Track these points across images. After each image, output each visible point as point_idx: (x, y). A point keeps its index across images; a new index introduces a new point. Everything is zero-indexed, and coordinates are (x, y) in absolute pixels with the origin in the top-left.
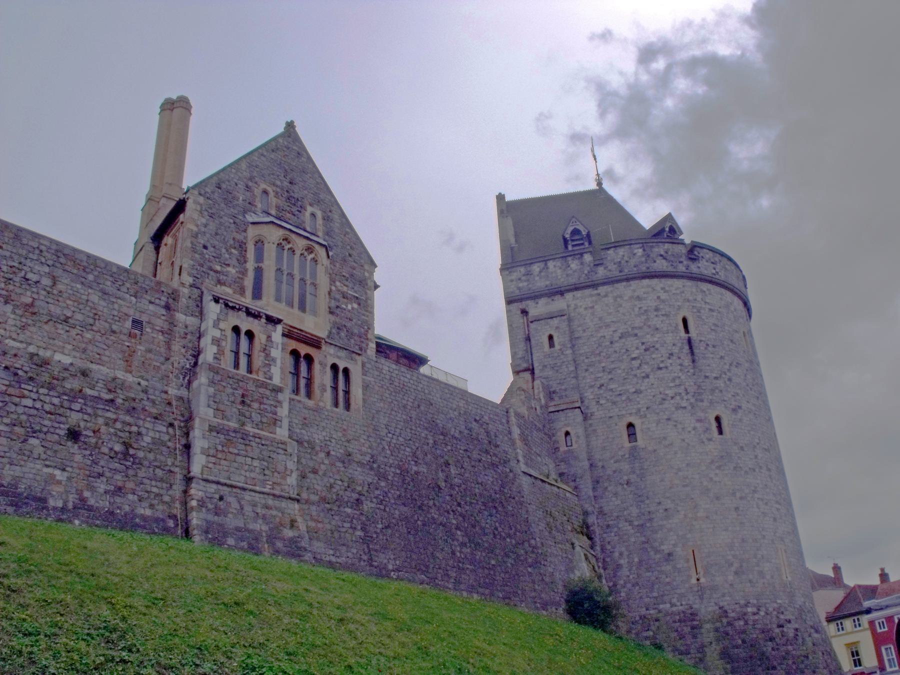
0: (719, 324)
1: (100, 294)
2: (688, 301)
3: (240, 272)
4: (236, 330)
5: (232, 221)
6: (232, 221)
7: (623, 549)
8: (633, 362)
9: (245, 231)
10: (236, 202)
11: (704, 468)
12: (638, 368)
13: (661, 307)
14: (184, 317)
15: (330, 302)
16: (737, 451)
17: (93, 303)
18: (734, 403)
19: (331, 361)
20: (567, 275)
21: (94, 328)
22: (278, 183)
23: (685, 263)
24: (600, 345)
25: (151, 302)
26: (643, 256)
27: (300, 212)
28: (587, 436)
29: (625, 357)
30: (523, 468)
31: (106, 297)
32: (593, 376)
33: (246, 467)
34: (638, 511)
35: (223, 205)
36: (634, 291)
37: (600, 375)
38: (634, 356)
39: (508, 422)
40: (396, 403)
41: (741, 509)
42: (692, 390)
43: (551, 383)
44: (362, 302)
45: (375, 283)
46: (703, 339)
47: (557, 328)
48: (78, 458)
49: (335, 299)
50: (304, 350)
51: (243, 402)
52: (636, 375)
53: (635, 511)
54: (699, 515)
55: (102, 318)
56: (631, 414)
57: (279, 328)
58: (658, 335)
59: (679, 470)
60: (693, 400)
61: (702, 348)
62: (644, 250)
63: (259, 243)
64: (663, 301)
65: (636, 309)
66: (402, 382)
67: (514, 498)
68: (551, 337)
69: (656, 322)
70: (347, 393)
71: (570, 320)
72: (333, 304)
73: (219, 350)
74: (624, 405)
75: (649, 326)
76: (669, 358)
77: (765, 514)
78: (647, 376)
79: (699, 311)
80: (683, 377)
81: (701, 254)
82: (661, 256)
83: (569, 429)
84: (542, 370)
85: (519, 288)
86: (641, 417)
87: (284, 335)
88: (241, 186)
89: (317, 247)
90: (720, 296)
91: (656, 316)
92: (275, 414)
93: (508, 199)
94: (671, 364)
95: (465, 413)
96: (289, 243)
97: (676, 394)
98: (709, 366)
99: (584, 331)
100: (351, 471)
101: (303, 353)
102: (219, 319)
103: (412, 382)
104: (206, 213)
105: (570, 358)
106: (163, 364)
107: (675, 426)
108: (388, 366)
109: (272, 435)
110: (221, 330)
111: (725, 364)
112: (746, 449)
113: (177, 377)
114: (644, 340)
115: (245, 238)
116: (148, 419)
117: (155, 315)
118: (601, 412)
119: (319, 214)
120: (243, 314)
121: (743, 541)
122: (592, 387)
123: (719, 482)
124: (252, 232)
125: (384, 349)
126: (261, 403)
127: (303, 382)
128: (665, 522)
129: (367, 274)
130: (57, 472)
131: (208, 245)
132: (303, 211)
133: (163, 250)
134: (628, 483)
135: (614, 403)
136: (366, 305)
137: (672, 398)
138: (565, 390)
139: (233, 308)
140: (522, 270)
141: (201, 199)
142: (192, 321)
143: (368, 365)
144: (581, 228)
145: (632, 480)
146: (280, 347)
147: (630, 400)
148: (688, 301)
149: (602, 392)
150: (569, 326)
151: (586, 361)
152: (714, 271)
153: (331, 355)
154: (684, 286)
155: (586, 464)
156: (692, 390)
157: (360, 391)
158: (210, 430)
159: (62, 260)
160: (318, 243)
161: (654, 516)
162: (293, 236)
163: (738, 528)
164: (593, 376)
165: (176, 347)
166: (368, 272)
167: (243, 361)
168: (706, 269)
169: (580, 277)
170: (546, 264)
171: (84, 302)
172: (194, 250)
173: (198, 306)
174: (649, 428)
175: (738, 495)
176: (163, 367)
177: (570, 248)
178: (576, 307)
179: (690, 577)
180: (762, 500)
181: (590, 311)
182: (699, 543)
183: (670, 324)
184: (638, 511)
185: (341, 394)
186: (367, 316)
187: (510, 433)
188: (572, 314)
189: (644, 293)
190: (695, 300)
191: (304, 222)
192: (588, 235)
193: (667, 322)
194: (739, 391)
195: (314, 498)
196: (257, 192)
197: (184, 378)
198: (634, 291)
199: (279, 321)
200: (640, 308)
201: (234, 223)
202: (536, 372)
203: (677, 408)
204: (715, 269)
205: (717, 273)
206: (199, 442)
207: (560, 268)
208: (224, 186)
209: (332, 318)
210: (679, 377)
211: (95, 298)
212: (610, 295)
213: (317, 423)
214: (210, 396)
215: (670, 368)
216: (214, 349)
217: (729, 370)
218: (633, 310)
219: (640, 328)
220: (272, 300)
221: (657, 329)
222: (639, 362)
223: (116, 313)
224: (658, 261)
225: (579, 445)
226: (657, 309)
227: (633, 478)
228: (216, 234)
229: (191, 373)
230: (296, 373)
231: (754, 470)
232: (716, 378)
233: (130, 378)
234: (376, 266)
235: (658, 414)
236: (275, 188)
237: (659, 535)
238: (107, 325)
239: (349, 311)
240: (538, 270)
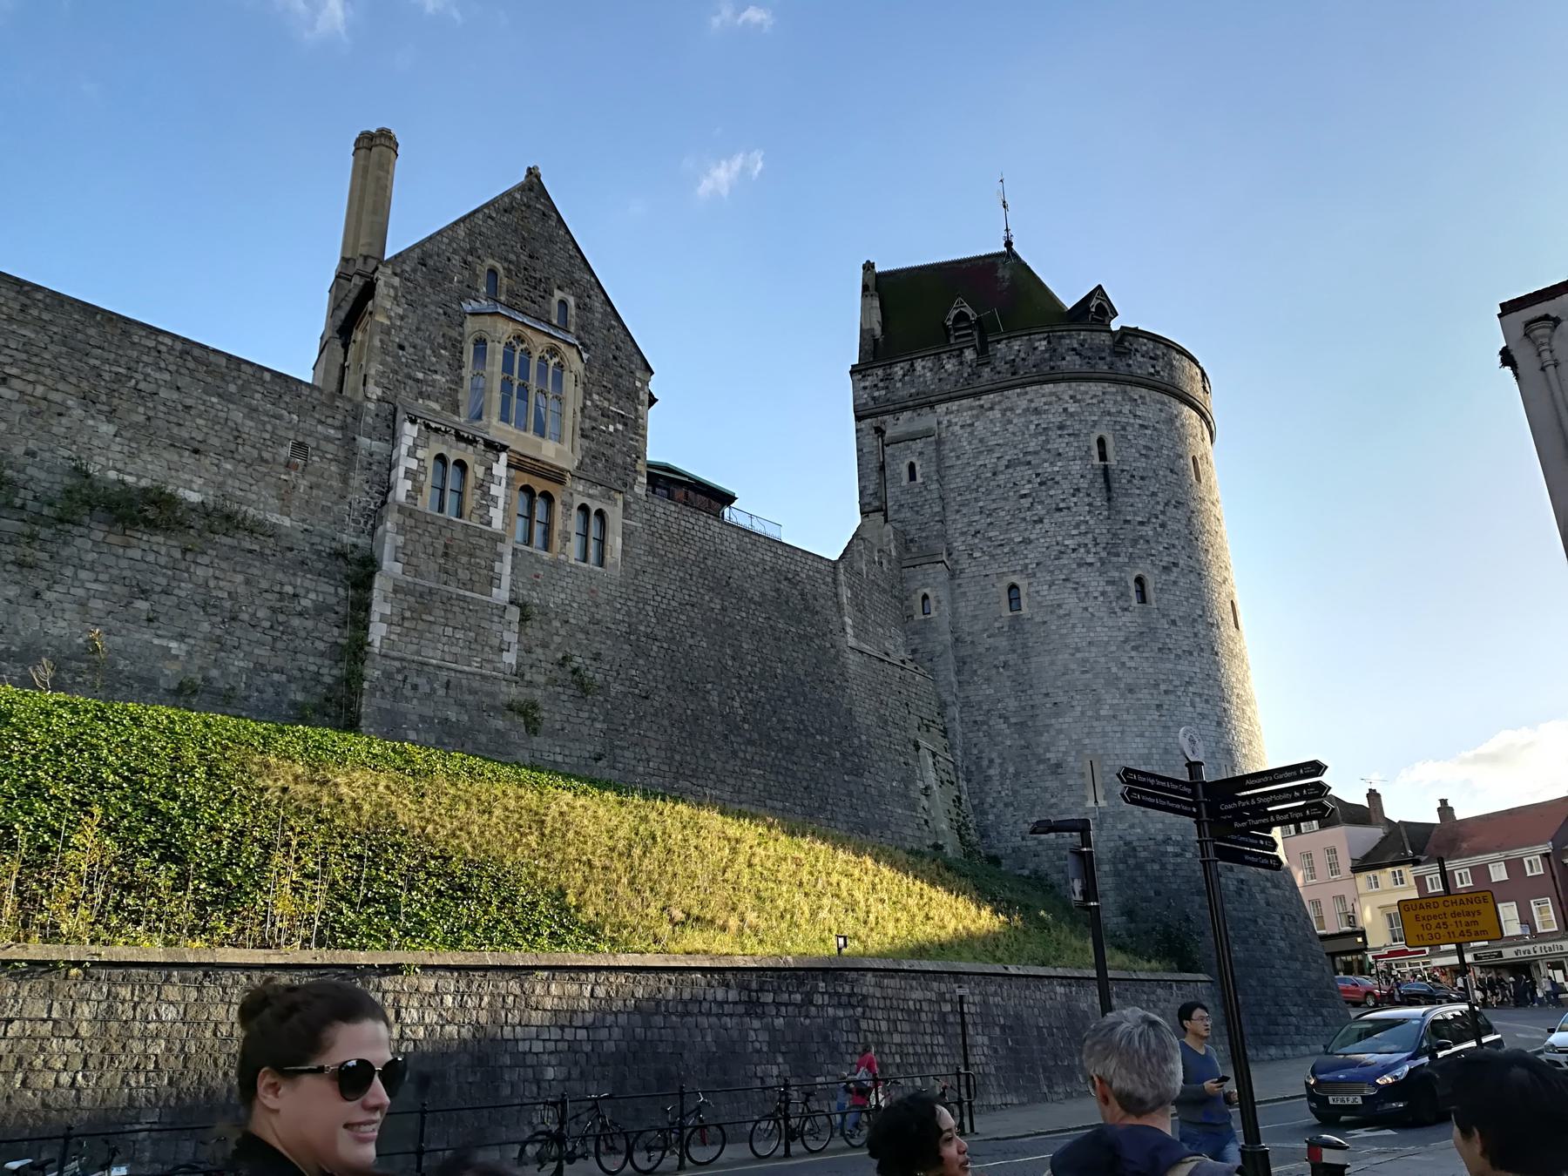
0: (1154, 446)
1: (246, 411)
2: (1109, 414)
3: (452, 381)
4: (441, 458)
5: (441, 311)
6: (441, 311)
7: (994, 755)
8: (1022, 501)
9: (461, 325)
10: (447, 285)
11: (1114, 648)
12: (1029, 509)
13: (1068, 423)
14: (368, 441)
15: (583, 422)
16: (1166, 626)
18: (1166, 559)
19: (579, 500)
20: (940, 380)
21: (236, 456)
22: (512, 257)
23: (1108, 359)
24: (978, 477)
25: (320, 422)
26: (1046, 351)
27: (543, 298)
28: (953, 601)
29: (1011, 494)
30: (852, 642)
31: (255, 415)
32: (966, 520)
33: (444, 640)
34: (1016, 704)
35: (429, 289)
36: (1031, 401)
37: (976, 518)
38: (1023, 492)
39: (835, 581)
40: (670, 555)
41: (1165, 707)
42: (1102, 540)
43: (908, 528)
44: (629, 422)
45: (651, 394)
46: (1127, 468)
47: (921, 453)
48: (206, 627)
49: (590, 418)
50: (539, 485)
51: (446, 555)
52: (1024, 519)
53: (1012, 704)
54: (1102, 713)
55: (249, 443)
56: (1014, 572)
57: (503, 456)
58: (1059, 464)
59: (1078, 650)
60: (1104, 554)
61: (1124, 481)
62: (1049, 342)
63: (480, 343)
64: (1072, 415)
65: (1032, 427)
67: (833, 682)
68: (912, 467)
69: (1058, 444)
70: (602, 542)
71: (939, 442)
72: (588, 424)
73: (413, 486)
74: (1006, 560)
75: (1049, 451)
76: (1074, 495)
77: (1203, 716)
78: (1041, 521)
79: (1124, 429)
80: (1091, 522)
81: (1135, 346)
82: (1074, 349)
83: (927, 591)
84: (897, 511)
85: (874, 398)
86: (1028, 576)
87: (509, 466)
88: (456, 260)
89: (563, 346)
90: (1159, 406)
91: (1060, 436)
92: (493, 570)
93: (878, 269)
94: (1075, 504)
95: (772, 569)
96: (523, 342)
97: (1079, 545)
98: (1132, 505)
99: (958, 457)
100: (596, 645)
101: (538, 491)
102: (415, 445)
103: (696, 528)
104: (403, 300)
105: (936, 495)
106: (337, 504)
107: (1076, 589)
108: (664, 509)
109: (484, 598)
110: (419, 460)
111: (1158, 503)
112: (1179, 624)
113: (357, 522)
114: (1040, 471)
115: (461, 335)
116: (309, 576)
117: (327, 439)
118: (974, 569)
119: (571, 301)
121: (1166, 751)
122: (963, 534)
123: (1136, 669)
124: (471, 325)
125: (667, 481)
126: (471, 555)
127: (538, 530)
128: (1053, 721)
129: (638, 384)
130: (173, 645)
131: (406, 344)
132: (547, 296)
133: (352, 348)
134: (1005, 665)
135: (992, 556)
136: (636, 428)
137: (1074, 550)
138: (927, 538)
139: (437, 430)
140: (880, 372)
141: (396, 281)
142: (377, 446)
143: (634, 506)
144: (969, 310)
145: (1011, 663)
146: (504, 482)
147: (1015, 553)
148: (1109, 414)
149: (977, 541)
150: (938, 451)
151: (959, 498)
152: (1152, 370)
153: (579, 493)
154: (1104, 393)
155: (948, 638)
156: (1102, 540)
157: (619, 541)
158: (395, 591)
159: (191, 365)
160: (565, 342)
161: (1038, 712)
162: (529, 332)
163: (1159, 734)
164: (966, 520)
165: (357, 479)
166: (640, 380)
167: (450, 499)
168: (1140, 368)
169: (957, 382)
170: (912, 365)
171: (222, 421)
172: (385, 351)
173: (388, 427)
174: (1037, 592)
175: (1163, 687)
176: (336, 509)
177: (952, 341)
178: (950, 424)
179: (1085, 798)
180: (1200, 695)
181: (969, 430)
182: (1101, 752)
183: (1079, 447)
184: (1016, 704)
185: (593, 544)
187: (836, 595)
188: (944, 435)
189: (1045, 404)
190: (1120, 412)
191: (549, 312)
192: (978, 321)
193: (1076, 444)
194: (1176, 542)
195: (542, 679)
196: (482, 270)
197: (366, 523)
198: (1031, 401)
199: (504, 448)
200: (1037, 425)
201: (445, 314)
202: (890, 513)
203: (1079, 565)
204: (1153, 367)
205: (1158, 372)
206: (380, 607)
207: (931, 370)
208: (431, 263)
209: (586, 443)
210: (1087, 522)
211: (238, 416)
212: (997, 407)
213: (553, 581)
214: (397, 547)
215: (1074, 510)
216: (409, 484)
217: (1163, 513)
218: (1028, 428)
219: (1036, 453)
220: (495, 421)
221: (1060, 454)
222: (1030, 500)
223: (267, 436)
224: (1068, 358)
225: (940, 613)
226: (1061, 427)
227: (1012, 658)
228: (418, 329)
229: (373, 518)
230: (530, 517)
231: (1191, 654)
232: (1141, 523)
233: (287, 522)
234: (652, 373)
235: (1052, 572)
236: (506, 265)
237: (1045, 738)
238: (255, 453)
239: (610, 434)
240: (901, 372)
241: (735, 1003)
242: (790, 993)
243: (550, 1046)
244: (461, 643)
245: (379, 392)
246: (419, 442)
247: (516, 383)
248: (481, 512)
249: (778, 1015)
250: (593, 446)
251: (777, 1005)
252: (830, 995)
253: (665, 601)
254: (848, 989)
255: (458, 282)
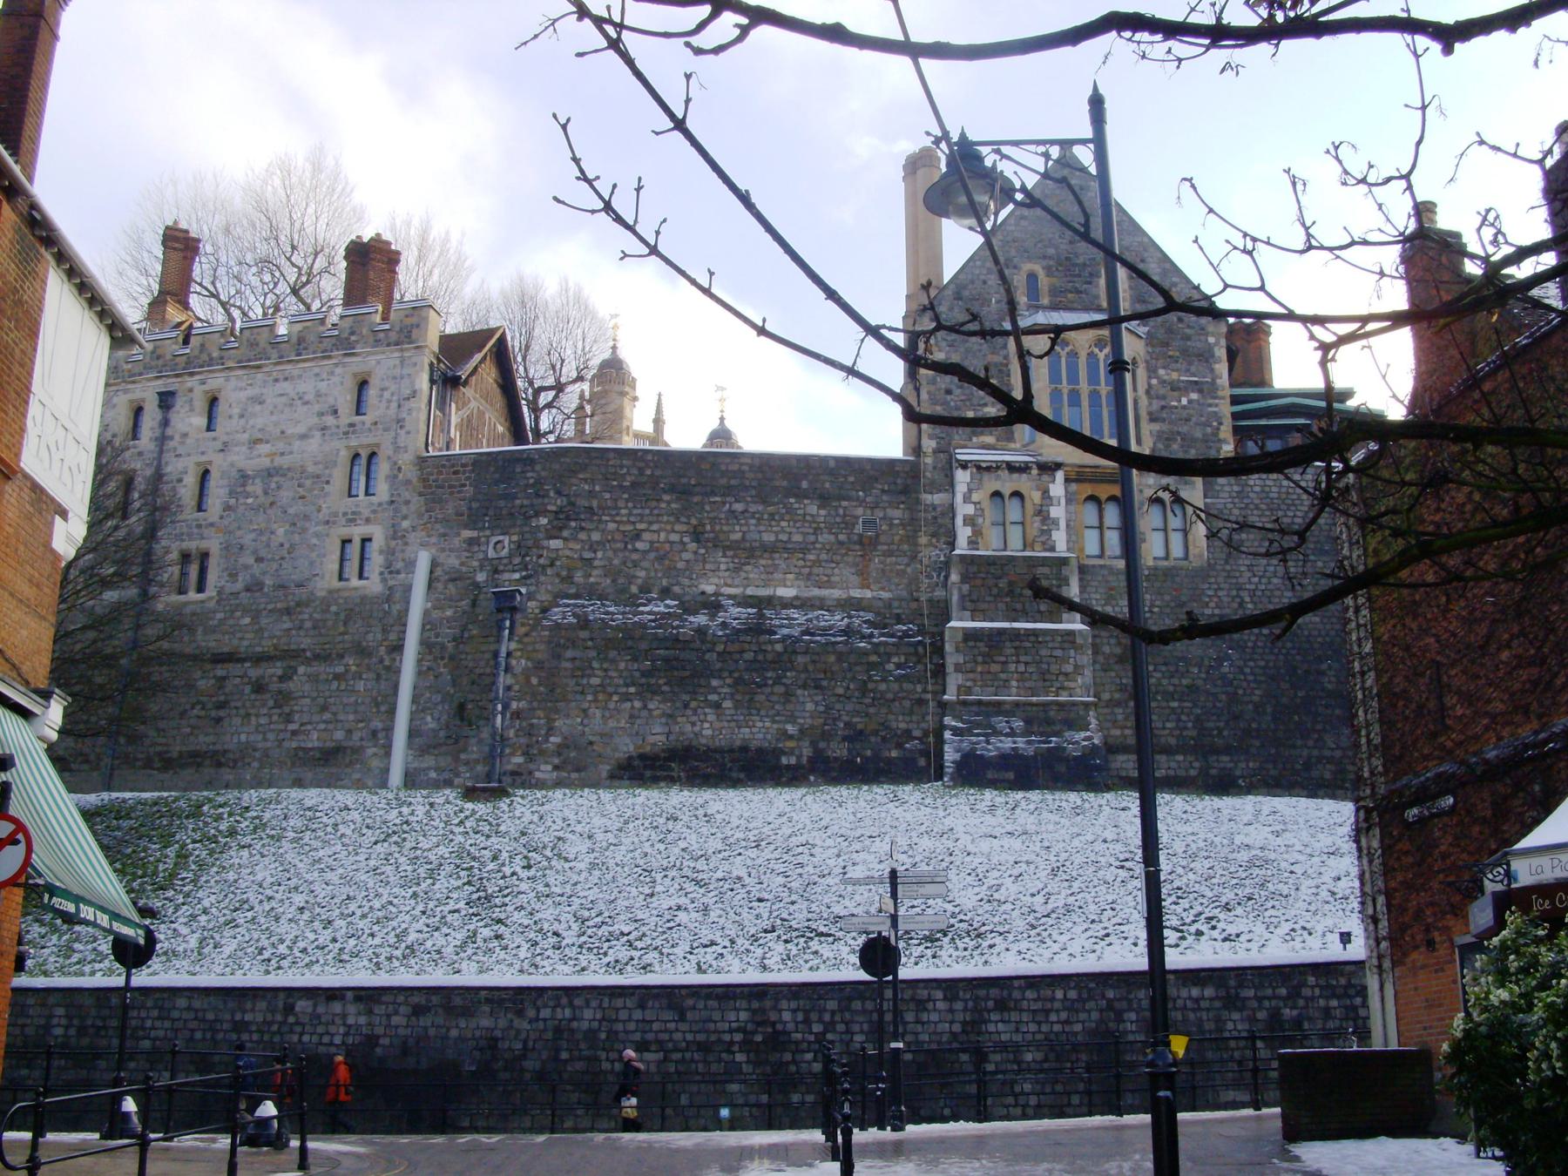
15: (1150, 404)
17: (812, 516)
44: (1205, 387)
49: (1158, 398)
57: (1060, 475)
66: (1284, 490)
72: (1156, 405)
73: (973, 532)
87: (1067, 480)
102: (970, 491)
110: (975, 503)
120: (1005, 474)
139: (988, 469)
146: (1063, 501)
173: (946, 476)
176: (909, 570)
186: (1217, 405)
197: (939, 576)
199: (1058, 466)
208: (966, 293)
209: (1156, 427)
216: (968, 531)
236: (1045, 263)
239: (1184, 407)
241: (1211, 999)
242: (1274, 988)
243: (1029, 1037)
244: (1035, 677)
245: (933, 444)
246: (972, 486)
247: (1065, 392)
248: (1043, 539)
249: (1261, 1008)
250: (1165, 427)
251: (1260, 999)
252: (1321, 988)
253: (1264, 580)
254: (1343, 981)
255: (997, 302)
